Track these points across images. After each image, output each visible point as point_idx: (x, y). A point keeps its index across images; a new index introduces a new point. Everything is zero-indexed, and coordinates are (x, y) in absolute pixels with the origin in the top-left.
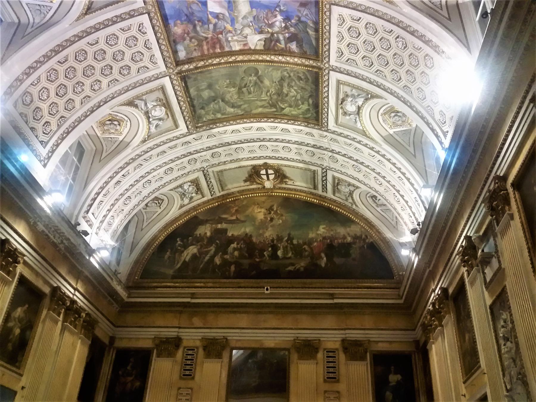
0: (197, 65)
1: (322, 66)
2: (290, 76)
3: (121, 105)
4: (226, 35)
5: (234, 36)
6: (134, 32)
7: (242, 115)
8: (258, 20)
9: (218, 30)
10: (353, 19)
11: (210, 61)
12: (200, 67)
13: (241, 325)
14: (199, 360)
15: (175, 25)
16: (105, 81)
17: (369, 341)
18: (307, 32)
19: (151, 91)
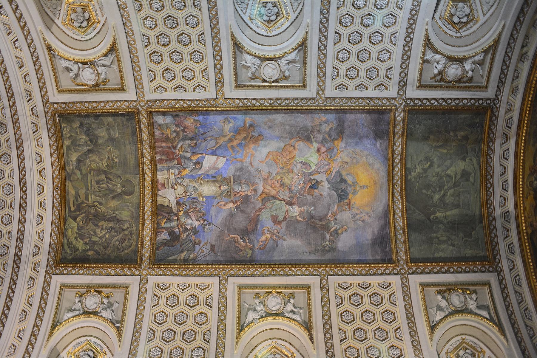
0: (144, 132)
2: (124, 230)
3: (114, 39)
6: (199, 80)
7: (66, 170)
8: (193, 202)
9: (183, 160)
15: (195, 121)
18: (182, 252)
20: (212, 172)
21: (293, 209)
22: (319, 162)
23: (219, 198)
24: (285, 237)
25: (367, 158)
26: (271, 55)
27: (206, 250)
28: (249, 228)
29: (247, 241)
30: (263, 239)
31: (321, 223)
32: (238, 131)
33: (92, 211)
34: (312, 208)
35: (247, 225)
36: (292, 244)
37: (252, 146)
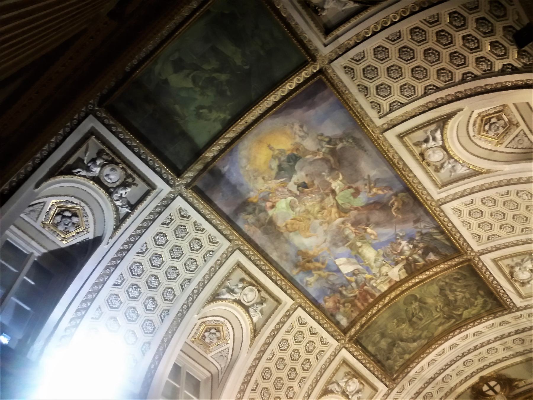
1: (469, 257)
2: (447, 283)
4: (369, 283)
5: (377, 280)
6: (297, 328)
7: (428, 343)
8: (388, 255)
9: (361, 284)
10: (468, 205)
11: (370, 313)
12: (364, 323)
15: (325, 302)
16: (295, 385)
18: (436, 239)
19: (337, 370)
20: (354, 260)
21: (336, 187)
22: (281, 199)
23: (370, 242)
24: (366, 177)
25: (246, 167)
26: (239, 308)
27: (422, 225)
28: (378, 207)
29: (391, 202)
30: (380, 192)
31: (331, 159)
32: (308, 271)
33: (446, 309)
34: (324, 174)
35: (377, 210)
36: (369, 168)
37: (311, 253)
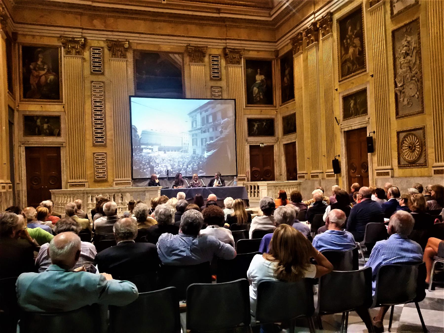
13: (141, 30)
14: (106, 59)
17: (244, 49)
